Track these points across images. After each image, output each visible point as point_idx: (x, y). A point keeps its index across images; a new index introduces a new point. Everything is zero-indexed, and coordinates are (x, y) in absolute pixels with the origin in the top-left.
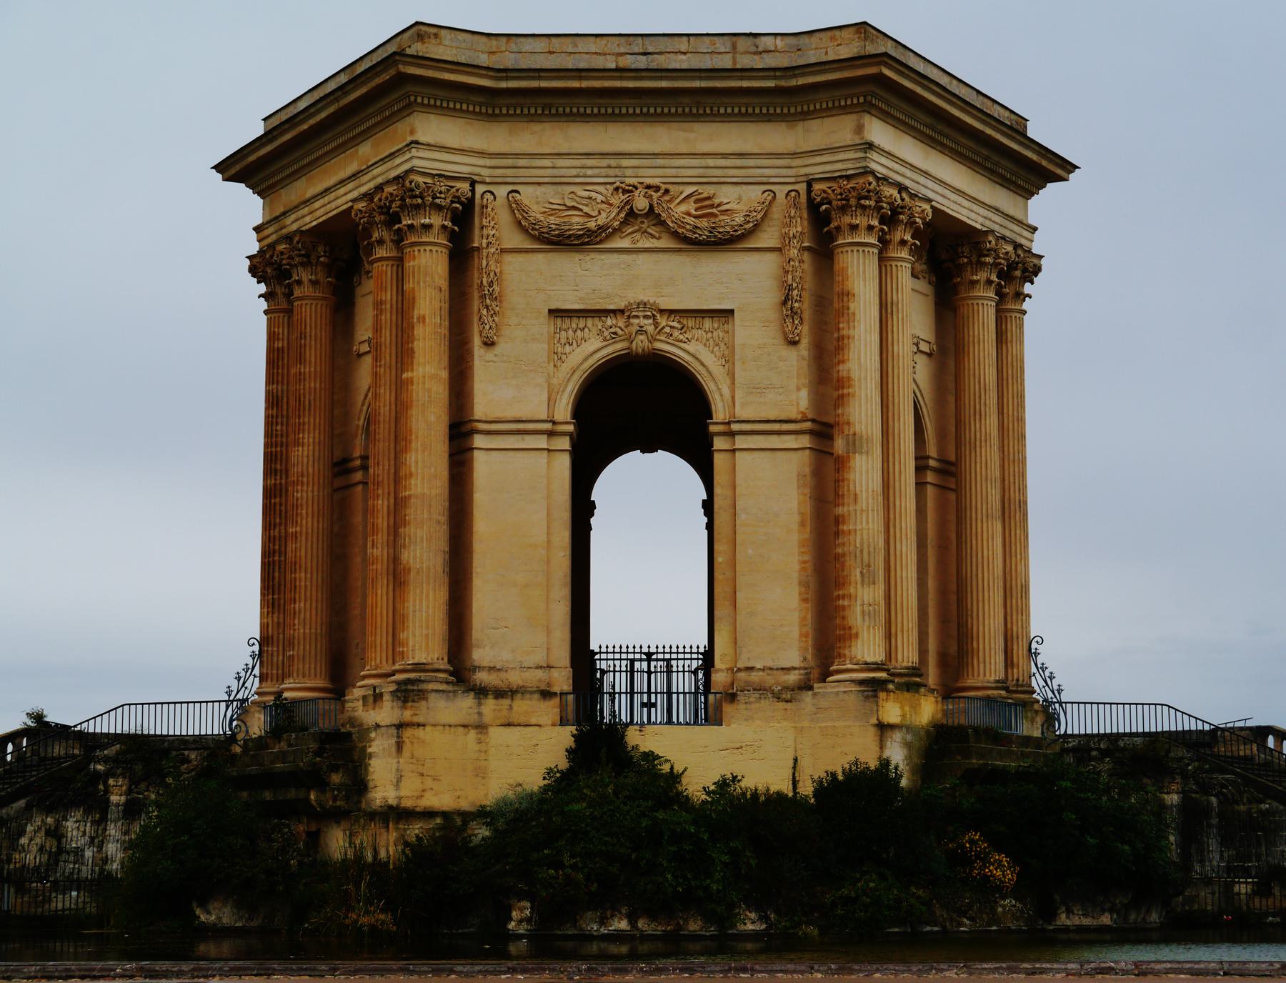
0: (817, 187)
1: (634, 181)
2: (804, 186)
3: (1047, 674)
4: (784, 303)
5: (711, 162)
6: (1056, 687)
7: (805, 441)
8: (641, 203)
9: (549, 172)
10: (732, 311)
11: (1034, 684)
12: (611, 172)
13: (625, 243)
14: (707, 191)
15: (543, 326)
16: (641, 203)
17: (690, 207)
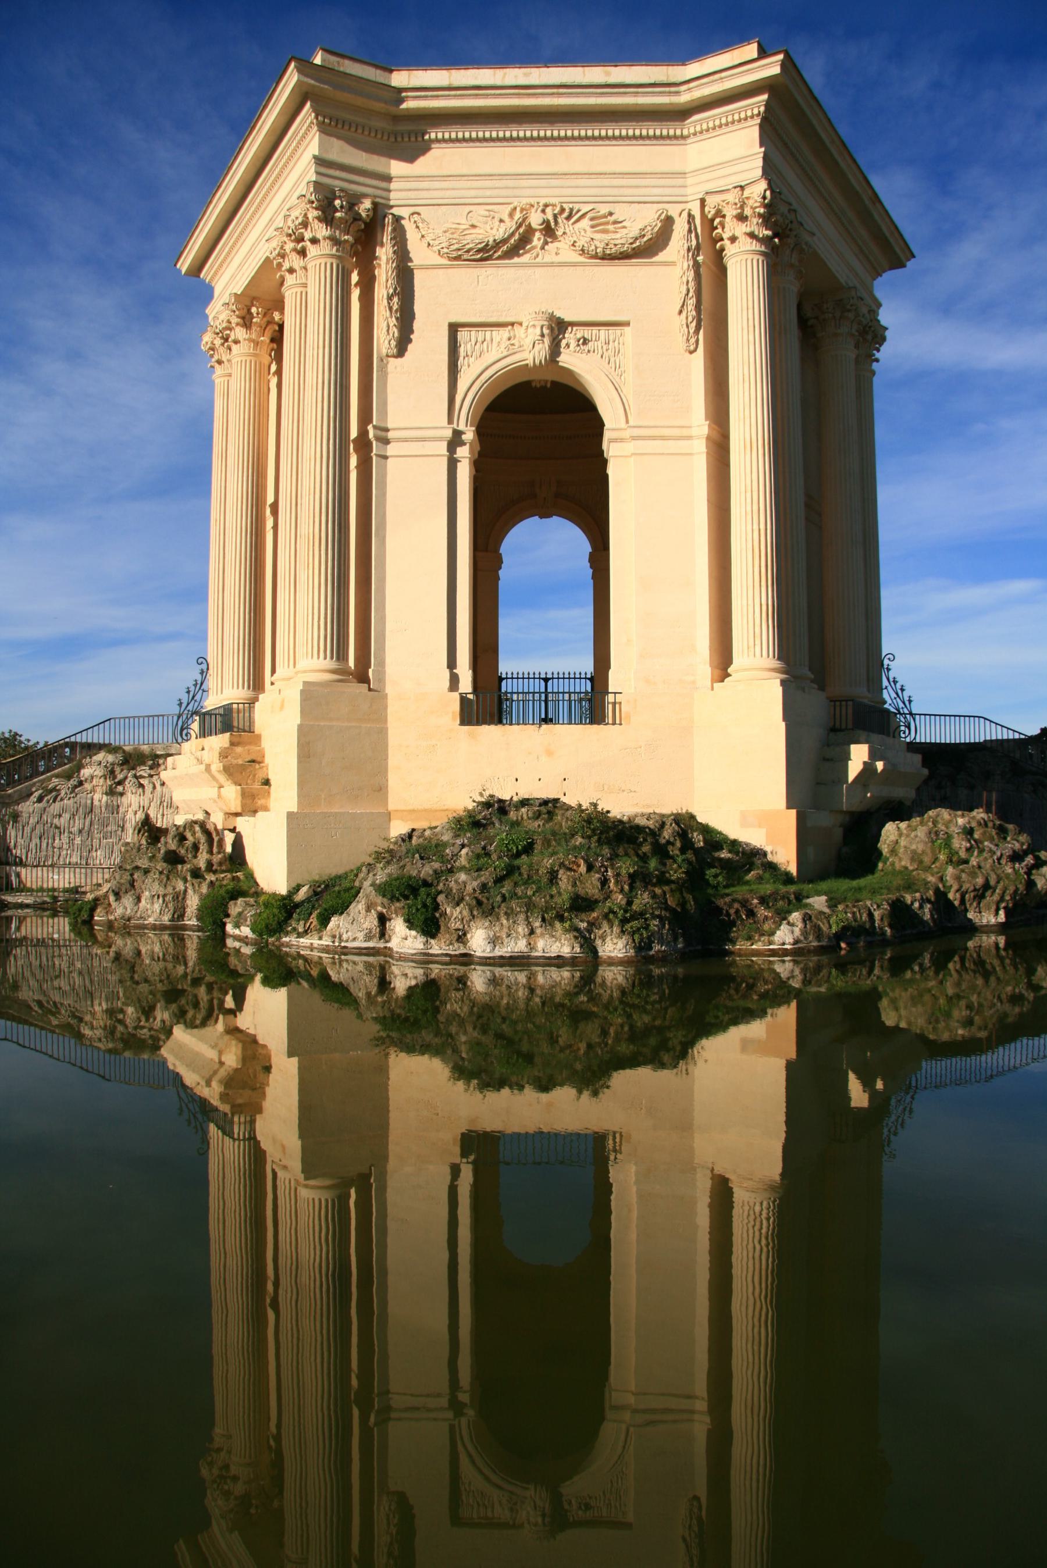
0: (712, 202)
1: (533, 201)
2: (698, 202)
3: (898, 686)
4: (680, 312)
5: (606, 182)
6: (906, 699)
9: (448, 193)
11: (885, 695)
12: (509, 192)
14: (604, 209)
16: (535, 220)
17: (585, 223)
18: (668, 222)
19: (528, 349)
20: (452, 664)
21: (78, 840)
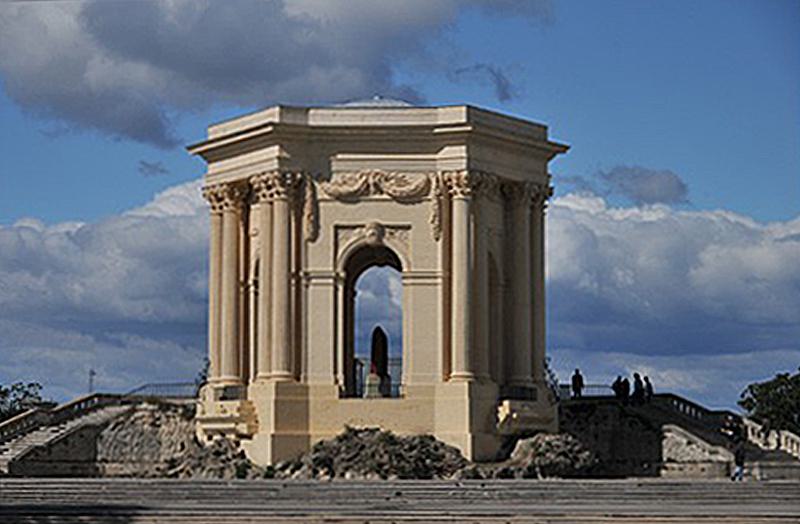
7: (440, 281)
17: (392, 181)
18: (429, 182)
19: (368, 236)
20: (335, 372)
21: (136, 449)
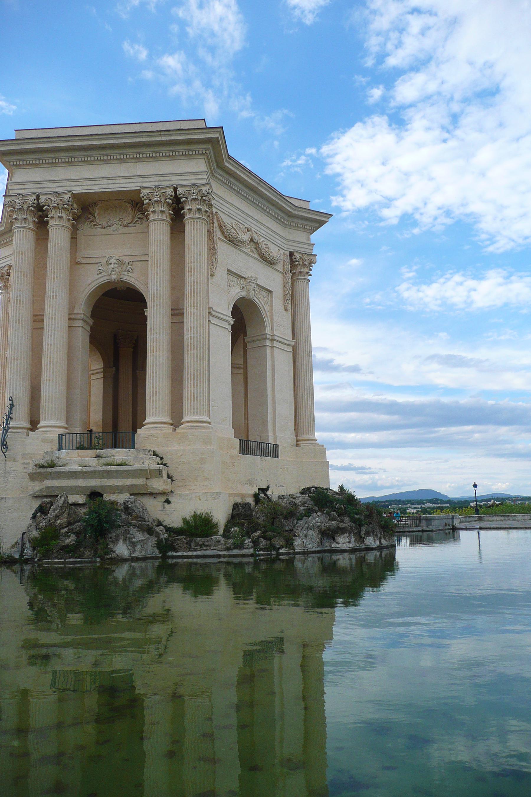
8: (256, 237)
9: (228, 210)
10: (271, 292)
13: (246, 251)
15: (225, 275)
